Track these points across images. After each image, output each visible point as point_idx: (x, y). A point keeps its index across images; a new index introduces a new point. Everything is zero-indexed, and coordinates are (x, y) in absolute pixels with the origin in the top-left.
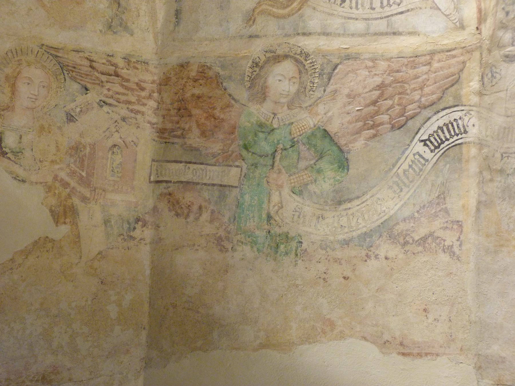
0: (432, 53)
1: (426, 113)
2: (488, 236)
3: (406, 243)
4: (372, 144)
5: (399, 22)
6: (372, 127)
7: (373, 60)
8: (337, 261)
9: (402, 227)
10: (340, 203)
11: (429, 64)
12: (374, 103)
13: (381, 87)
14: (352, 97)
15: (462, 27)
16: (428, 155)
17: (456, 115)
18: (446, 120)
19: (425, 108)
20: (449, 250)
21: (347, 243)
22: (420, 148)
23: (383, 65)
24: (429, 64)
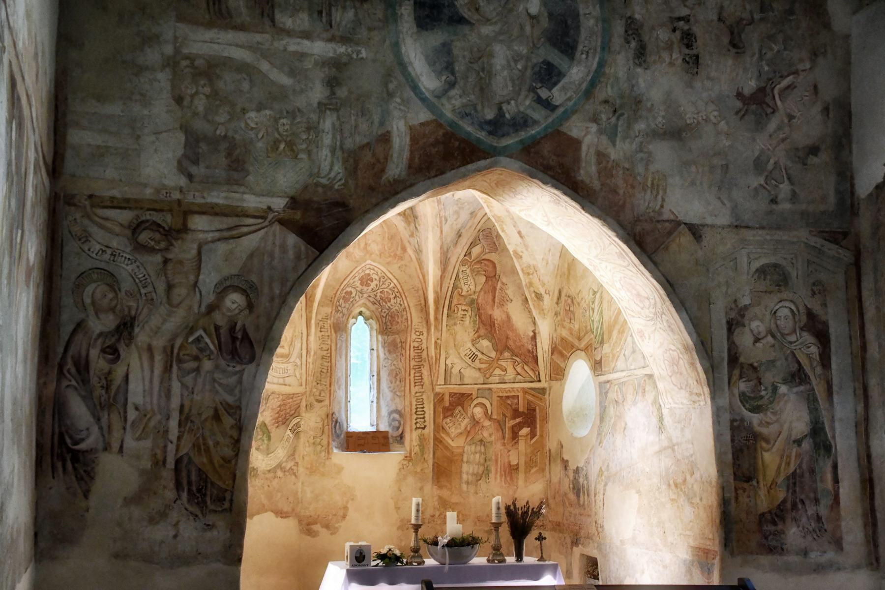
0: (294, 394)
1: (291, 418)
2: (307, 468)
3: (285, 471)
4: (278, 430)
5: (288, 380)
6: (278, 422)
7: (279, 394)
8: (267, 479)
9: (283, 465)
10: (268, 454)
11: (292, 398)
12: (278, 413)
13: (280, 406)
14: (273, 409)
15: (301, 385)
16: (291, 435)
17: (299, 420)
18: (296, 422)
19: (291, 416)
20: (295, 474)
21: (269, 471)
22: (289, 432)
23: (281, 397)
24: (292, 398)
